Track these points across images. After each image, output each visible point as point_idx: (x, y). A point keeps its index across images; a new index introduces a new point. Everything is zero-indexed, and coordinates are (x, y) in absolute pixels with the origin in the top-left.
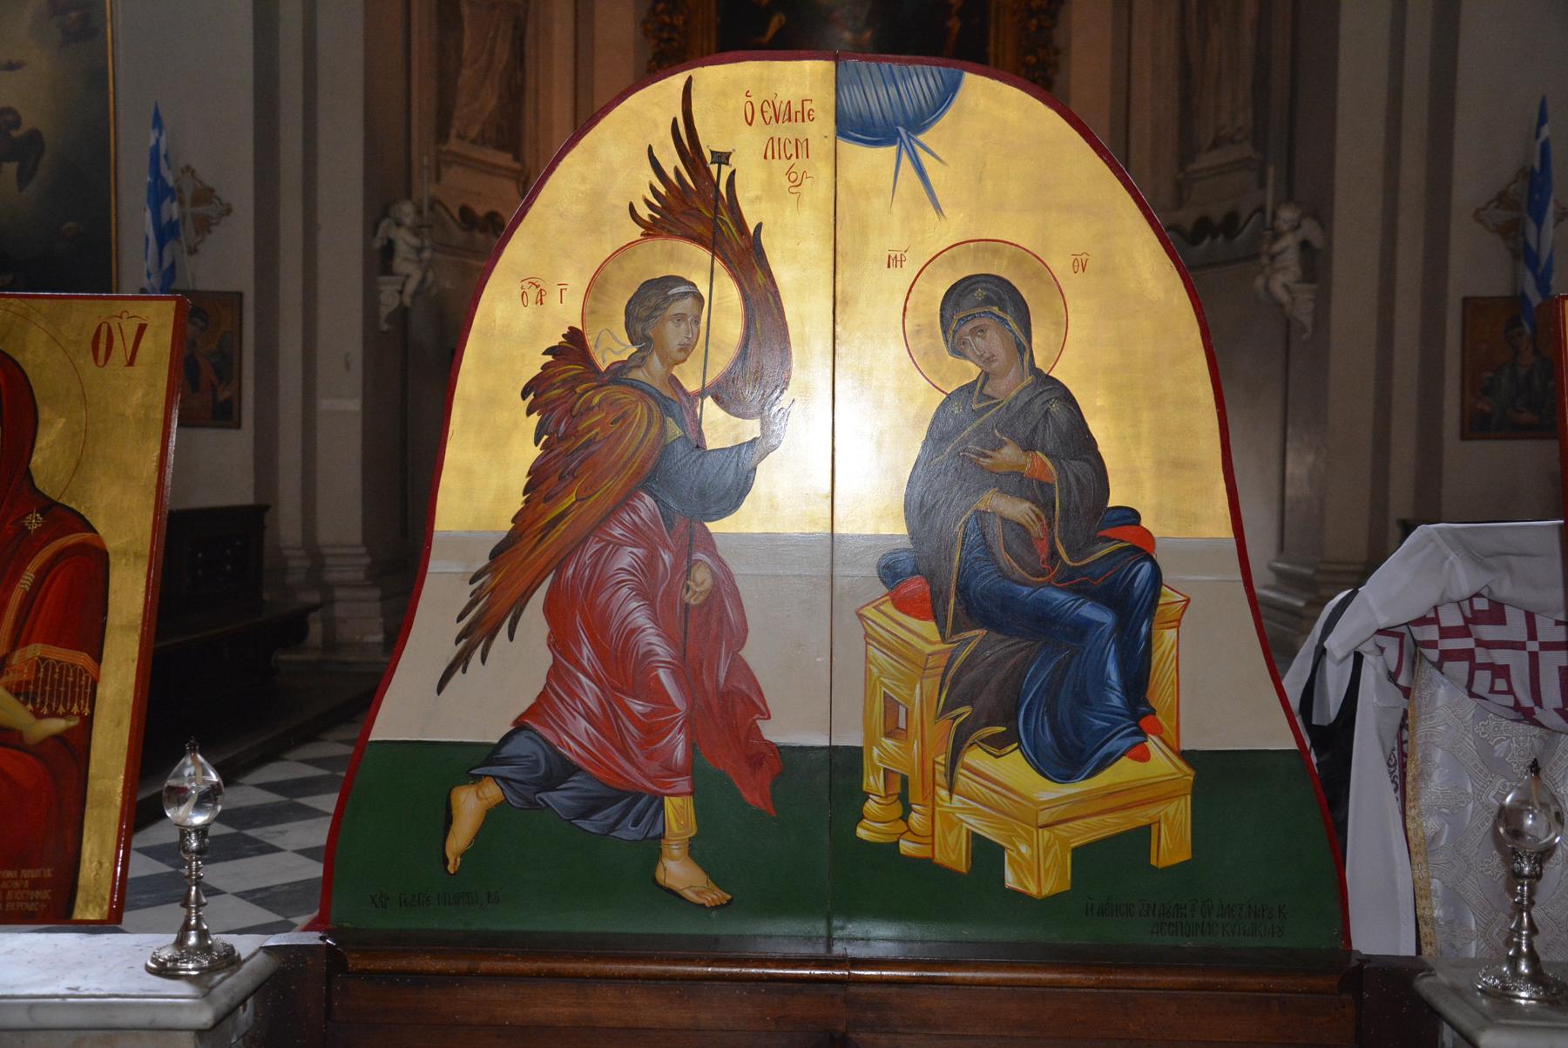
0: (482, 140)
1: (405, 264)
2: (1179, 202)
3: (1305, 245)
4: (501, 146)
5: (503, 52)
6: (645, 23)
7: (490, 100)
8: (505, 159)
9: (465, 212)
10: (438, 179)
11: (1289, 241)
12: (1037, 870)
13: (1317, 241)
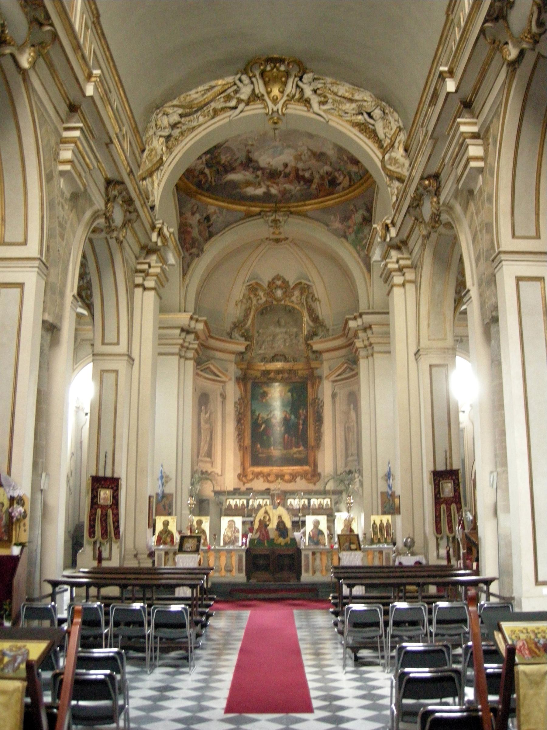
0: (205, 456)
2: (346, 466)
3: (360, 480)
4: (208, 457)
5: (208, 438)
7: (206, 448)
8: (208, 459)
9: (202, 471)
11: (357, 480)
12: (283, 544)
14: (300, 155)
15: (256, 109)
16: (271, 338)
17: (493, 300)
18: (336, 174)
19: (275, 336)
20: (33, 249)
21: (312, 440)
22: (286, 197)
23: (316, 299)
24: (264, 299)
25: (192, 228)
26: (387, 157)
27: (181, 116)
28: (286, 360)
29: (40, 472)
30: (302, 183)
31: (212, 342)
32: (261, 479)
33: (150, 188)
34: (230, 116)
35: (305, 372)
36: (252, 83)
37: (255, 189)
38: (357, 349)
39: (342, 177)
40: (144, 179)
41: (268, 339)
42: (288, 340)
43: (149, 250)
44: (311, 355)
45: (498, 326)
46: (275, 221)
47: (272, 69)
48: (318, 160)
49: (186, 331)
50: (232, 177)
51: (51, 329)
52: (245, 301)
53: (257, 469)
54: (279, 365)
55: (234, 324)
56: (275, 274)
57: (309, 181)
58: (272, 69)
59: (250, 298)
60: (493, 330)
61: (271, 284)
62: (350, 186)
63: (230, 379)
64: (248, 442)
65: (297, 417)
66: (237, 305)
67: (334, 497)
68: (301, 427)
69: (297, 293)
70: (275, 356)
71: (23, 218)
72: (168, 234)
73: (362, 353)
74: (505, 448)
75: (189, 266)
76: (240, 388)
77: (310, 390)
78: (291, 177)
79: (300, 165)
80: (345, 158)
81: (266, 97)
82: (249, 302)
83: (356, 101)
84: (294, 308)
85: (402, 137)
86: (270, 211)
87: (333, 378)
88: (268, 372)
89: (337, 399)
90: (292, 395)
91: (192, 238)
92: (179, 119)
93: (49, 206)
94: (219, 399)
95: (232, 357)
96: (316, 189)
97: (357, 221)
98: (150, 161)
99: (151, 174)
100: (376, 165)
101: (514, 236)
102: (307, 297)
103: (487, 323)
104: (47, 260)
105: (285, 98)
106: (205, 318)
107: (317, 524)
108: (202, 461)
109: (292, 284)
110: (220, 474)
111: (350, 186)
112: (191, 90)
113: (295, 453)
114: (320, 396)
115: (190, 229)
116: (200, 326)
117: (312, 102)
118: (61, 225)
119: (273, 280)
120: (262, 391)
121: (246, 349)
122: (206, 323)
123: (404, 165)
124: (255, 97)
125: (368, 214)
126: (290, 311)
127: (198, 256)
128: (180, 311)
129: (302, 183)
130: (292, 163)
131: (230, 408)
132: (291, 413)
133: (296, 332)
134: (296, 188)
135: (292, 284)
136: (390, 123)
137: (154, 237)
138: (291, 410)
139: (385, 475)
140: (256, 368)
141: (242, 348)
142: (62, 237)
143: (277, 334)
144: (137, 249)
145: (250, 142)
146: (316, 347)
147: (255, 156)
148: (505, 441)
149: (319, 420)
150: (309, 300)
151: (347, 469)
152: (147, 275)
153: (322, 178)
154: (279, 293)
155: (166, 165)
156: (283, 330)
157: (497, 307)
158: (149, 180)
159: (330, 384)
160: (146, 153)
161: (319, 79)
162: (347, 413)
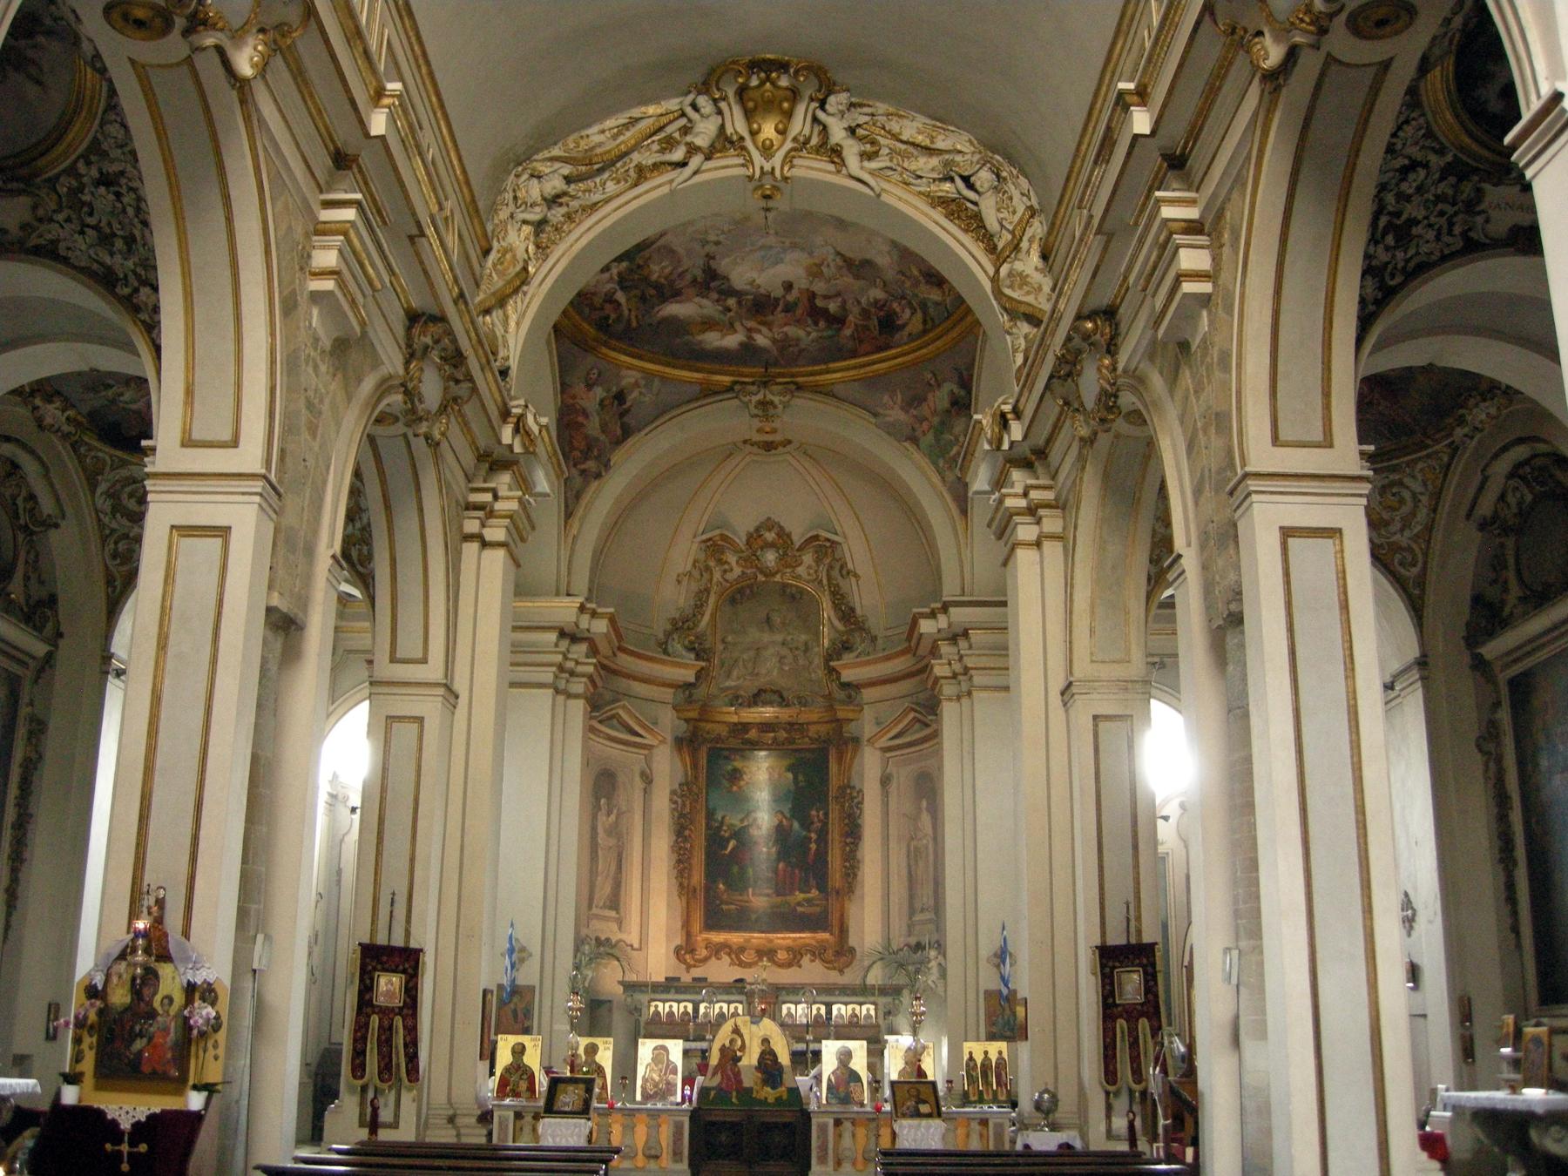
0: (604, 907)
4: (611, 908)
5: (613, 867)
7: (608, 889)
8: (613, 914)
9: (597, 939)
11: (933, 964)
12: (771, 1100)
14: (819, 266)
15: (728, 167)
16: (752, 653)
17: (1232, 576)
18: (895, 305)
20: (250, 455)
22: (787, 353)
24: (737, 571)
26: (1004, 270)
27: (568, 180)
28: (783, 701)
29: (252, 933)
30: (822, 324)
31: (625, 661)
32: (726, 959)
33: (499, 331)
34: (672, 181)
35: (823, 729)
36: (720, 112)
37: (723, 336)
38: (937, 679)
39: (908, 312)
40: (487, 312)
41: (745, 656)
42: (790, 659)
43: (494, 462)
44: (840, 695)
45: (1242, 632)
46: (764, 404)
47: (762, 83)
48: (857, 277)
49: (569, 635)
50: (674, 309)
51: (284, 626)
52: (696, 574)
53: (718, 937)
54: (767, 712)
55: (674, 622)
56: (762, 519)
57: (838, 321)
58: (762, 83)
59: (708, 569)
60: (1231, 641)
61: (754, 537)
62: (925, 332)
63: (663, 742)
64: (698, 877)
65: (806, 824)
67: (882, 1000)
68: (813, 846)
69: (808, 558)
70: (761, 691)
71: (231, 390)
72: (535, 429)
73: (948, 689)
74: (1258, 898)
75: (578, 497)
77: (833, 767)
78: (799, 312)
79: (819, 287)
80: (916, 273)
81: (749, 143)
83: (940, 152)
84: (802, 591)
85: (1038, 228)
86: (753, 383)
87: (883, 742)
88: (745, 727)
90: (795, 778)
91: (586, 437)
92: (565, 187)
93: (287, 365)
94: (639, 784)
95: (668, 694)
96: (852, 336)
97: (939, 408)
98: (501, 274)
99: (502, 302)
100: (981, 287)
101: (1276, 440)
102: (831, 567)
103: (1219, 627)
104: (280, 481)
105: (789, 145)
106: (611, 610)
107: (845, 1057)
108: (597, 917)
109: (797, 540)
110: (636, 945)
111: (925, 332)
112: (589, 126)
113: (799, 904)
114: (855, 782)
115: (580, 419)
116: (601, 626)
117: (845, 153)
118: (310, 405)
119: (757, 530)
121: (698, 676)
122: (612, 620)
123: (1040, 289)
124: (724, 142)
125: (963, 393)
126: (793, 597)
127: (598, 476)
128: (557, 594)
129: (822, 324)
130: (802, 283)
131: (662, 804)
132: (793, 816)
134: (809, 334)
135: (797, 540)
136: (1011, 198)
137: (507, 434)
138: (793, 810)
139: (995, 955)
141: (689, 675)
142: (313, 431)
143: (766, 648)
144: (468, 458)
145: (712, 238)
146: (848, 675)
147: (723, 265)
148: (1255, 883)
149: (853, 833)
150: (835, 573)
151: (913, 941)
152: (491, 514)
153: (865, 313)
154: (770, 557)
155: (535, 282)
156: (779, 638)
157: (1240, 593)
158: (497, 314)
159: (878, 753)
160: (493, 257)
161: (861, 105)
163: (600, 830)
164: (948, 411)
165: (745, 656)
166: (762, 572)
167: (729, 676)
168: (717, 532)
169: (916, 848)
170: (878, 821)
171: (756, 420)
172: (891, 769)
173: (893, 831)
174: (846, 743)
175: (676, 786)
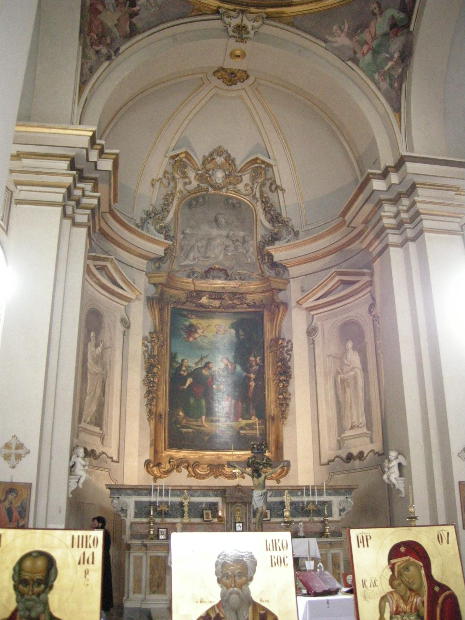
0: (90, 423)
1: (80, 471)
2: (340, 448)
3: (400, 465)
5: (99, 390)
6: (144, 380)
7: (94, 408)
8: (97, 429)
10: (77, 438)
13: (404, 463)
16: (204, 243)
19: (210, 240)
21: (273, 407)
23: (277, 187)
24: (195, 184)
25: (104, 7)
28: (227, 277)
32: (185, 472)
35: (257, 297)
38: (384, 229)
41: (200, 244)
42: (232, 248)
44: (269, 272)
46: (241, 29)
52: (165, 181)
53: (178, 454)
55: (148, 214)
56: (216, 146)
59: (174, 178)
61: (209, 159)
63: (137, 298)
64: (163, 406)
65: (247, 368)
66: (153, 185)
68: (253, 384)
69: (246, 178)
70: (211, 269)
73: (393, 238)
75: (92, 71)
76: (153, 314)
77: (267, 325)
82: (172, 184)
84: (240, 202)
86: (234, 10)
88: (199, 294)
89: (318, 338)
94: (120, 328)
95: (143, 263)
97: (379, 33)
102: (263, 184)
106: (117, 151)
108: (85, 430)
109: (239, 164)
110: (115, 458)
114: (285, 334)
115: (100, 7)
119: (211, 155)
120: (187, 323)
126: (234, 206)
127: (109, 58)
128: (72, 123)
132: (235, 362)
133: (244, 238)
135: (239, 164)
138: (235, 357)
140: (179, 285)
141: (159, 250)
143: (214, 239)
149: (285, 372)
150: (266, 189)
154: (219, 176)
156: (224, 233)
159: (304, 313)
162: (341, 358)
163: (89, 356)
164: (386, 35)
165: (200, 244)
166: (212, 186)
167: (187, 257)
168: (184, 150)
169: (343, 381)
170: (306, 363)
171: (233, 40)
172: (317, 322)
173: (320, 369)
174: (278, 307)
175: (147, 334)
